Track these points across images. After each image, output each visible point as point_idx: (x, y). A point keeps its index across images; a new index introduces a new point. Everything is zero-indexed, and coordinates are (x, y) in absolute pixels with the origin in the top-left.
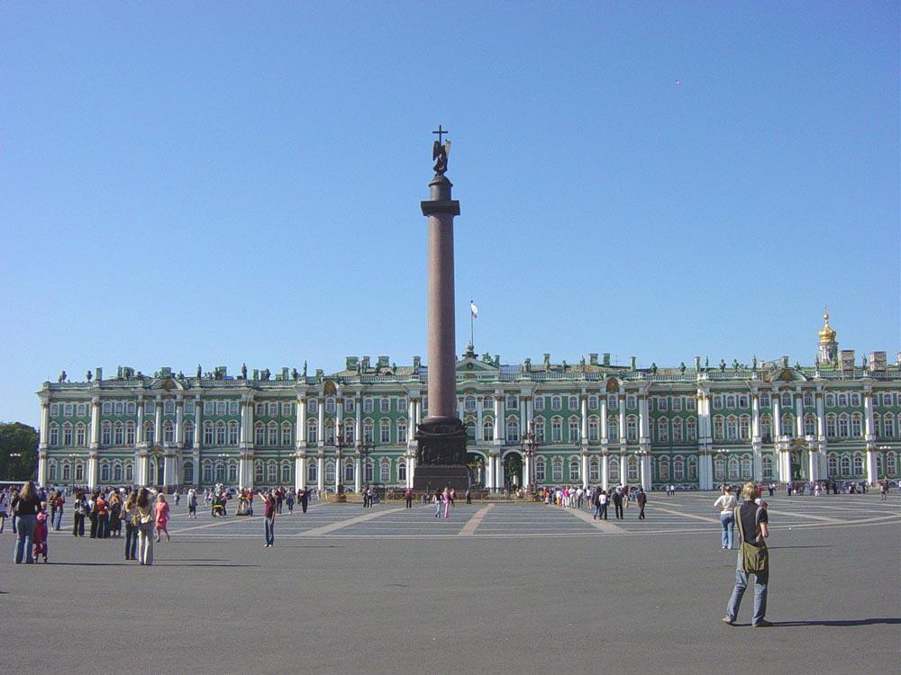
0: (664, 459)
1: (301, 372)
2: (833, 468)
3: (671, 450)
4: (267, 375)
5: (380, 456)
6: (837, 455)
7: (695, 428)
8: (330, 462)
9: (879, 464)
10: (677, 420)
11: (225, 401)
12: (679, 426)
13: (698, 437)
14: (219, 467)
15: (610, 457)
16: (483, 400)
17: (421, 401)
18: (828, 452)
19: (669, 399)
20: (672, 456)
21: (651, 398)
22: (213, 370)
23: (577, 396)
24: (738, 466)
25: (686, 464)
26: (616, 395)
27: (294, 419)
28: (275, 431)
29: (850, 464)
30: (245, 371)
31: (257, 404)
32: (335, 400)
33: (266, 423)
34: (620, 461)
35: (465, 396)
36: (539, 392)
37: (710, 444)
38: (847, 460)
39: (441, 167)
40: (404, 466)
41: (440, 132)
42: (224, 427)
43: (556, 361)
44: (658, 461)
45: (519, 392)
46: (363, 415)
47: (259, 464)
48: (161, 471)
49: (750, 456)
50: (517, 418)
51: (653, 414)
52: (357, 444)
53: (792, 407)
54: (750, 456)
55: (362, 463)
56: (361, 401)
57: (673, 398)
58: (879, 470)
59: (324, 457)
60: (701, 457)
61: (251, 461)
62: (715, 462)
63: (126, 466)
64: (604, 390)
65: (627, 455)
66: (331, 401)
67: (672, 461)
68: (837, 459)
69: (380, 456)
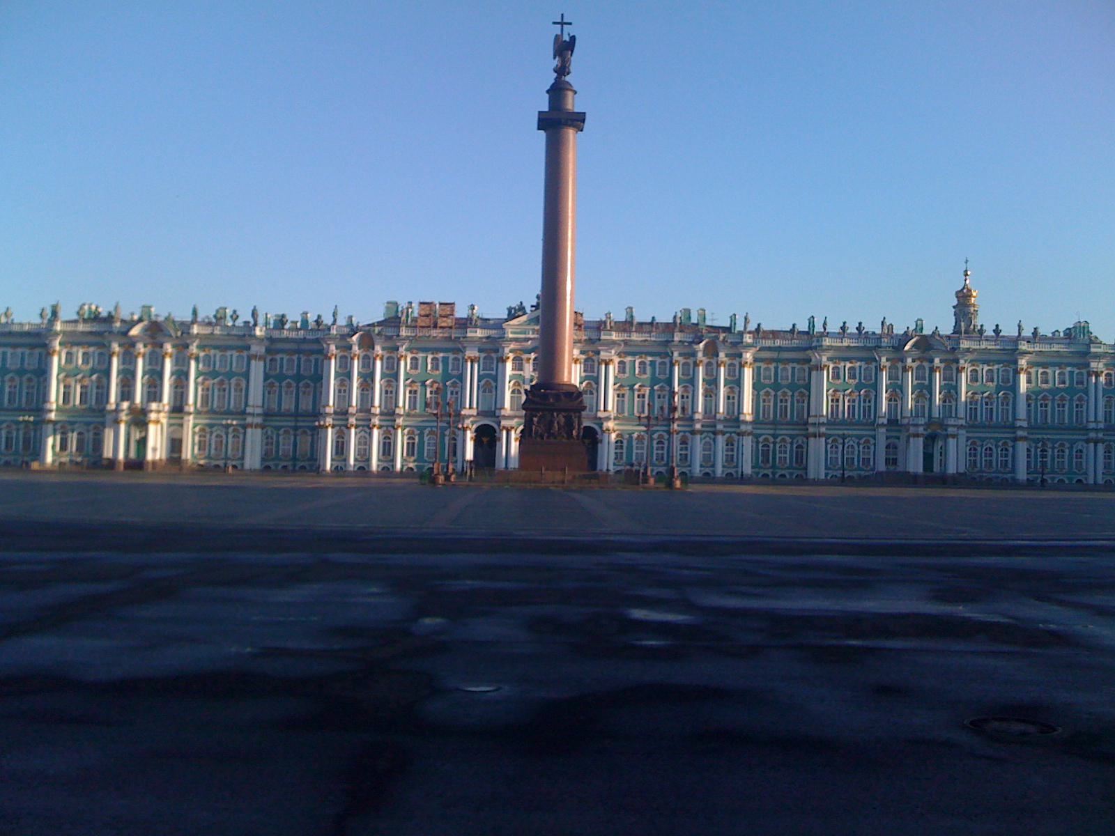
0: (766, 440)
1: (327, 320)
2: (972, 458)
3: (775, 429)
4: (281, 321)
5: (426, 427)
6: (979, 443)
7: (806, 405)
9: (1029, 456)
10: (785, 394)
11: (228, 353)
12: (786, 401)
13: (808, 415)
14: (217, 436)
15: (703, 436)
17: (479, 362)
18: (968, 439)
19: (776, 368)
20: (775, 436)
21: (758, 364)
22: (212, 314)
23: (667, 360)
24: (856, 453)
25: (792, 447)
26: (714, 361)
28: (292, 392)
29: (995, 455)
30: (254, 314)
31: (269, 358)
34: (714, 440)
35: (533, 356)
36: (619, 355)
37: (823, 424)
38: (991, 449)
39: (562, 71)
40: (455, 439)
41: (562, 24)
42: (226, 386)
43: (641, 316)
44: (758, 442)
45: (598, 353)
47: (269, 433)
48: (142, 442)
49: (872, 441)
50: (595, 386)
53: (927, 383)
54: (872, 441)
57: (781, 366)
58: (1028, 462)
60: (812, 440)
61: (259, 431)
62: (829, 446)
63: (91, 434)
64: (700, 355)
65: (724, 435)
67: (774, 443)
68: (979, 449)
69: (426, 427)
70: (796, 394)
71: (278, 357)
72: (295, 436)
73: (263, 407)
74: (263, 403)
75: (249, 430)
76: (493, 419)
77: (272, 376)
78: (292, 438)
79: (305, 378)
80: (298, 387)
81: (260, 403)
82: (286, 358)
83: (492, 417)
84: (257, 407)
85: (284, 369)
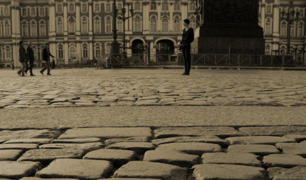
8: (72, 46)
16: (173, 5)
17: (132, 4)
21: (280, 8)
27: (47, 18)
28: (35, 26)
32: (74, 4)
33: (29, 21)
46: (93, 14)
51: (281, 19)
52: (91, 33)
55: (93, 46)
56: (92, 4)
59: (68, 42)
66: (71, 5)
69: (105, 42)
70: (299, 23)
71: (26, 8)
72: (39, 49)
73: (21, 34)
74: (21, 32)
75: (14, 47)
76: (141, 36)
77: (24, 18)
78: (37, 50)
79: (41, 18)
80: (38, 23)
81: (18, 32)
82: (30, 8)
83: (140, 35)
84: (17, 34)
85: (31, 13)
